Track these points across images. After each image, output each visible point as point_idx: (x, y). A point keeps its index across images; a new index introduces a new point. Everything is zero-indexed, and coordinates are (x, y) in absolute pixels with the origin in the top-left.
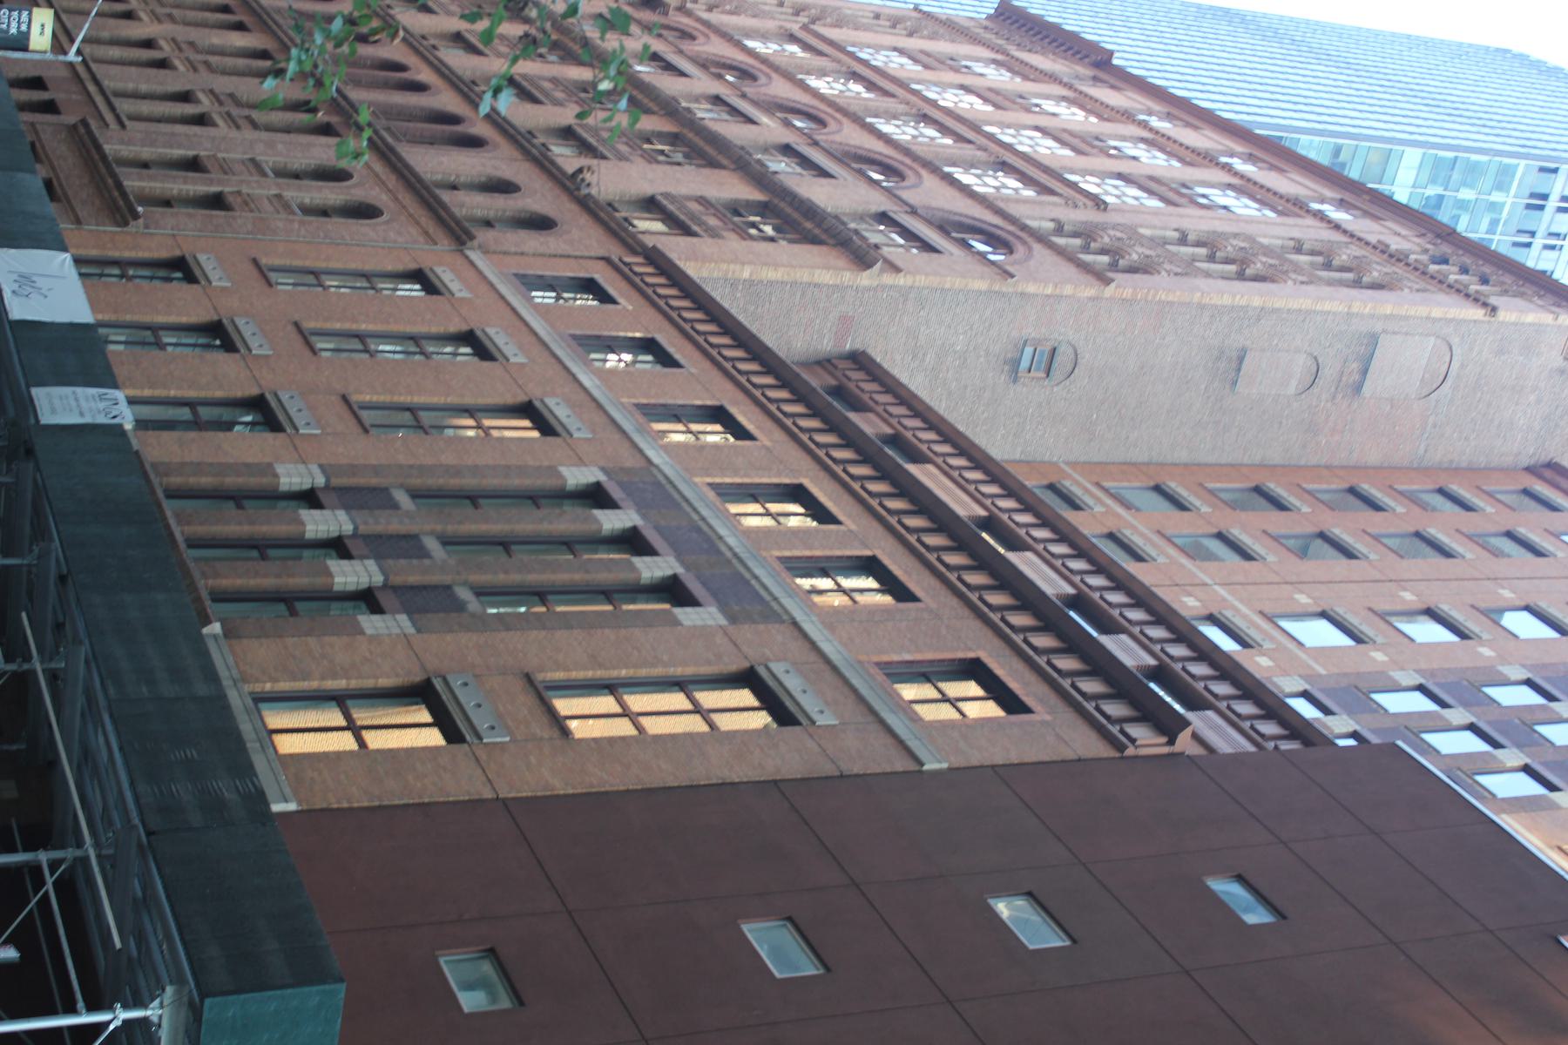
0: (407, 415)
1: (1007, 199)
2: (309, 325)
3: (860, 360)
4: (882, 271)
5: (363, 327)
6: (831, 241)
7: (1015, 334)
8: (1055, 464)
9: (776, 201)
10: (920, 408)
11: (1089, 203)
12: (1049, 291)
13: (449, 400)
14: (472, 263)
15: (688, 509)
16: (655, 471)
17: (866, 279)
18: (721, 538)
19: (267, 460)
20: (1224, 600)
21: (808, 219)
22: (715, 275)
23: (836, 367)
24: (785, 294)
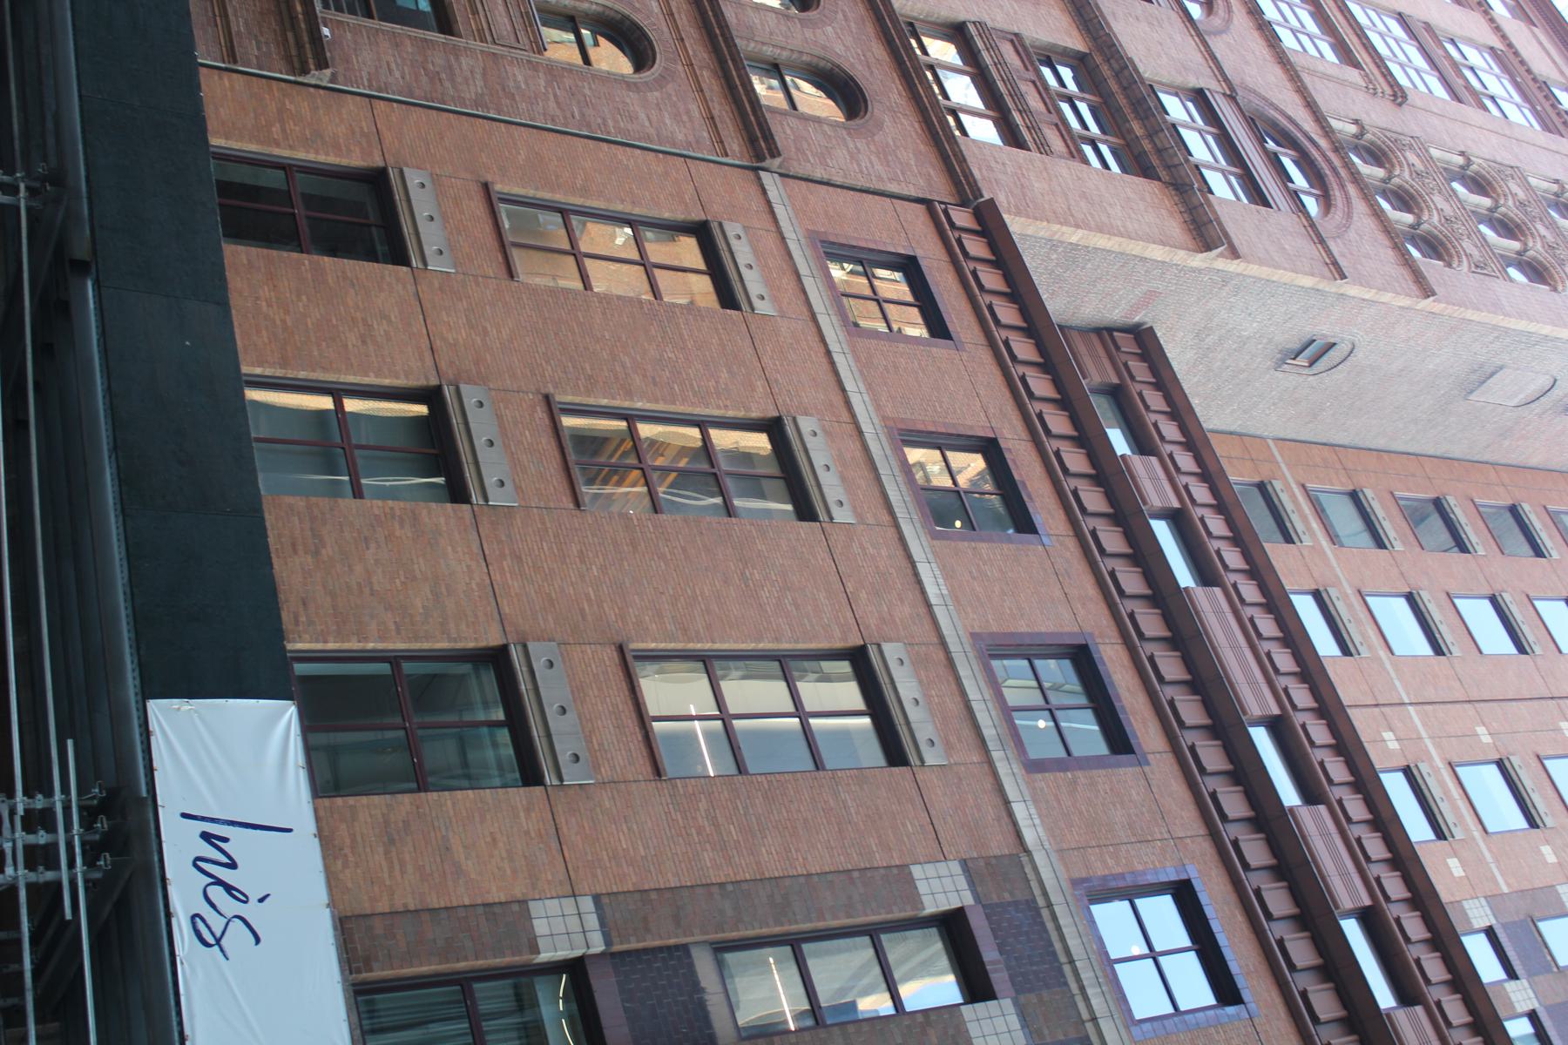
1: (1313, 73)
3: (1144, 340)
4: (1221, 255)
5: (639, 405)
6: (1163, 174)
9: (1098, 59)
10: (1212, 468)
11: (1388, 91)
12: (1367, 297)
13: (761, 646)
14: (764, 192)
15: (1074, 987)
16: (1025, 859)
17: (1199, 260)
19: (518, 892)
20: (1427, 752)
21: (1138, 117)
22: (1041, 234)
23: (1118, 348)
24: (1090, 241)
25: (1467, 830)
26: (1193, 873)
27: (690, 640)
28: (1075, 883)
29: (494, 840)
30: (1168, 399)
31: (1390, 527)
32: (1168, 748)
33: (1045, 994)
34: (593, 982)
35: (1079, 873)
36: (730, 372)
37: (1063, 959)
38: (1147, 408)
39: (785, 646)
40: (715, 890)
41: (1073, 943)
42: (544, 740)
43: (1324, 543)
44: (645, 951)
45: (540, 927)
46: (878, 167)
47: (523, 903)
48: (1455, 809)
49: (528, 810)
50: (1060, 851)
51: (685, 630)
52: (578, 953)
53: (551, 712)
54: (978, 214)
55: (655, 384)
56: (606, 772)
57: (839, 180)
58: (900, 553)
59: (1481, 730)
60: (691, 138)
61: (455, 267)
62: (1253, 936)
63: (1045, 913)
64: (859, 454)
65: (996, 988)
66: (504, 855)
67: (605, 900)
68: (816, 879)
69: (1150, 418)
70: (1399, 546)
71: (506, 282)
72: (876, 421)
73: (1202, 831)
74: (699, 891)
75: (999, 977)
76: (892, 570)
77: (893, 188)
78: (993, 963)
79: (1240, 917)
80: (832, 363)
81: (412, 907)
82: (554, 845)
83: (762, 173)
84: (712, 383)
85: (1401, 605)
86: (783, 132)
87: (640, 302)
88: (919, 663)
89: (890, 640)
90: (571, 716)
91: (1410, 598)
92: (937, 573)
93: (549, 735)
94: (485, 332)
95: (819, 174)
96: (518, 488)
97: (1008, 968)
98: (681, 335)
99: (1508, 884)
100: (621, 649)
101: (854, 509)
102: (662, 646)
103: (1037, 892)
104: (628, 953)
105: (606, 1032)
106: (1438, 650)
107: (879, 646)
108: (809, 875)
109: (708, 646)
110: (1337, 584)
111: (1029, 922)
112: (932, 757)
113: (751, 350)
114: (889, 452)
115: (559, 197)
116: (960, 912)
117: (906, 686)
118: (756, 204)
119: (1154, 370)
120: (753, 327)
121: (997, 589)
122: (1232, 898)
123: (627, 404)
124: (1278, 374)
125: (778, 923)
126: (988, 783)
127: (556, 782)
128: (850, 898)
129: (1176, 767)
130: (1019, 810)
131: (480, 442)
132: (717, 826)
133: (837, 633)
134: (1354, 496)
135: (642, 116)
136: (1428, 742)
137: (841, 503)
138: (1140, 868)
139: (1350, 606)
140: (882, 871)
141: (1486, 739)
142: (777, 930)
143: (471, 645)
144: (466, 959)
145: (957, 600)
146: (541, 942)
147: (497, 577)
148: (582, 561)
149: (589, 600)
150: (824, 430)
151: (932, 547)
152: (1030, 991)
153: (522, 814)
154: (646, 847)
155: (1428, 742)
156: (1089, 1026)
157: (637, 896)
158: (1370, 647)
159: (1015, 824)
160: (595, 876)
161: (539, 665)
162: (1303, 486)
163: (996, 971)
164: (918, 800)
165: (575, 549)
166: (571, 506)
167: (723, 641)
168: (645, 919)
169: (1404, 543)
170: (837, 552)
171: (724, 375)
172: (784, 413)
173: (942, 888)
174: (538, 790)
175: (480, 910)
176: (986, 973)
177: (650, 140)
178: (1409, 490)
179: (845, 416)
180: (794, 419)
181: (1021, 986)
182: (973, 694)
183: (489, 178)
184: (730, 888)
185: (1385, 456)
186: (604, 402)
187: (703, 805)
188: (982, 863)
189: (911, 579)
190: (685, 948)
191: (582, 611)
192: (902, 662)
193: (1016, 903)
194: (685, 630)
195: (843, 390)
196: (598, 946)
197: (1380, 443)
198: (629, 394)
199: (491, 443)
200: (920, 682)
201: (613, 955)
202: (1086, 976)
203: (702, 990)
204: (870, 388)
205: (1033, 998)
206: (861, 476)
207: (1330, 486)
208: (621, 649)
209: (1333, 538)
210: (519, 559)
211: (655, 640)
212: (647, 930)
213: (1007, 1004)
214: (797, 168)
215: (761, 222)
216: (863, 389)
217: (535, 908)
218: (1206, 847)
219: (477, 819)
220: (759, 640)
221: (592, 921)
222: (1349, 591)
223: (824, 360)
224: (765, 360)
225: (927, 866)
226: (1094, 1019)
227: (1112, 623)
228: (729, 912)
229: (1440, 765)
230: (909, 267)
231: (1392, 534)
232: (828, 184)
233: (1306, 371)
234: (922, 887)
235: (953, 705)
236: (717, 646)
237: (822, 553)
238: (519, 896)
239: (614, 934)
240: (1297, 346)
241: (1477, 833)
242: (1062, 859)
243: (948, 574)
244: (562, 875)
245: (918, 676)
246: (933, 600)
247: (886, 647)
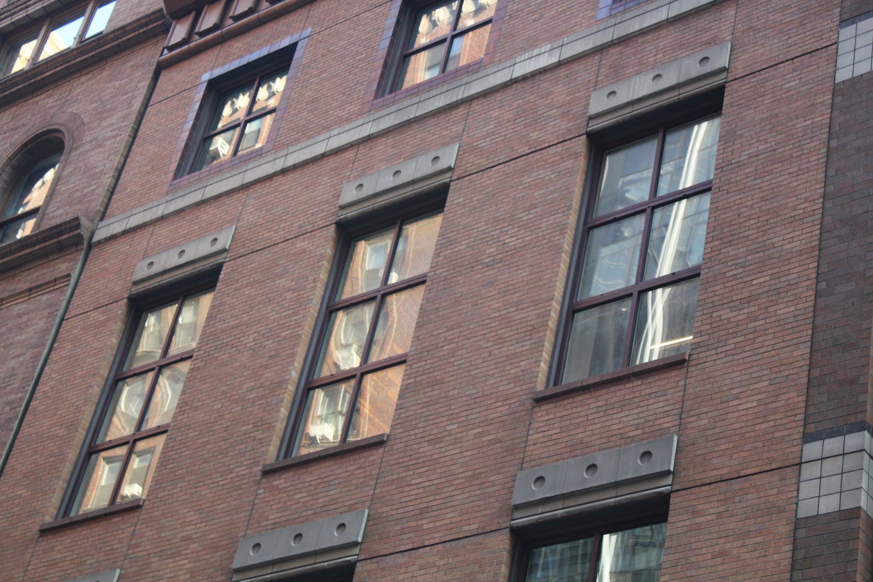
0: (581, 320)
2: (271, 454)
5: (294, 374)
13: (567, 247)
14: (113, 237)
19: (784, 528)
27: (545, 324)
29: (721, 554)
36: (280, 276)
39: (572, 220)
40: (822, 302)
45: (829, 505)
46: (115, 118)
47: (798, 524)
49: (695, 513)
53: (592, 481)
54: (178, 16)
55: (277, 356)
56: (668, 423)
57: (117, 160)
58: (499, 96)
60: (45, 313)
61: (113, 569)
64: (389, 140)
66: (740, 543)
67: (812, 428)
68: (830, 188)
71: (142, 515)
72: (361, 121)
74: (820, 320)
76: (515, 105)
77: (137, 104)
80: (295, 167)
82: (737, 485)
83: (95, 239)
84: (289, 295)
86: (59, 215)
87: (192, 370)
88: (617, 74)
89: (587, 106)
90: (599, 459)
92: (527, 55)
93: (617, 485)
94: (188, 539)
95: (107, 180)
96: (351, 508)
98: (237, 327)
100: (540, 400)
101: (444, 145)
102: (546, 356)
107: (591, 118)
108: (825, 196)
109: (556, 306)
112: (720, 59)
113: (264, 254)
114: (394, 108)
115: (72, 454)
118: (122, 246)
120: (242, 251)
123: (291, 388)
127: (669, 480)
131: (295, 548)
132: (749, 300)
133: (569, 164)
135: (12, 363)
137: (436, 158)
140: (836, 113)
143: (504, 569)
145: (560, 35)
146: (848, 505)
147: (438, 536)
148: (439, 440)
149: (480, 435)
150: (360, 176)
153: (698, 520)
154: (760, 379)
160: (782, 440)
161: (539, 493)
164: (764, 75)
165: (426, 448)
166: (381, 451)
170: (484, 163)
171: (282, 282)
172: (334, 219)
174: (674, 500)
177: (40, 355)
179: (350, 154)
180: (342, 208)
183: (36, 528)
184: (823, 285)
186: (284, 412)
187: (725, 314)
189: (528, 84)
191: (492, 442)
192: (613, 93)
194: (534, 329)
195: (323, 156)
198: (281, 384)
199: (299, 536)
200: (638, 73)
204: (327, 128)
206: (416, 135)
208: (540, 400)
210: (423, 511)
211: (538, 363)
214: (97, 205)
215: (141, 240)
216: (326, 135)
217: (806, 510)
219: (693, 572)
220: (559, 249)
221: (833, 445)
223: (291, 176)
224: (277, 238)
225: (840, 64)
230: (221, 90)
232: (120, 171)
235: (668, 37)
236: (558, 294)
237: (485, 180)
238: (789, 528)
243: (532, 43)
244: (774, 477)
246: (555, 59)
247: (593, 109)
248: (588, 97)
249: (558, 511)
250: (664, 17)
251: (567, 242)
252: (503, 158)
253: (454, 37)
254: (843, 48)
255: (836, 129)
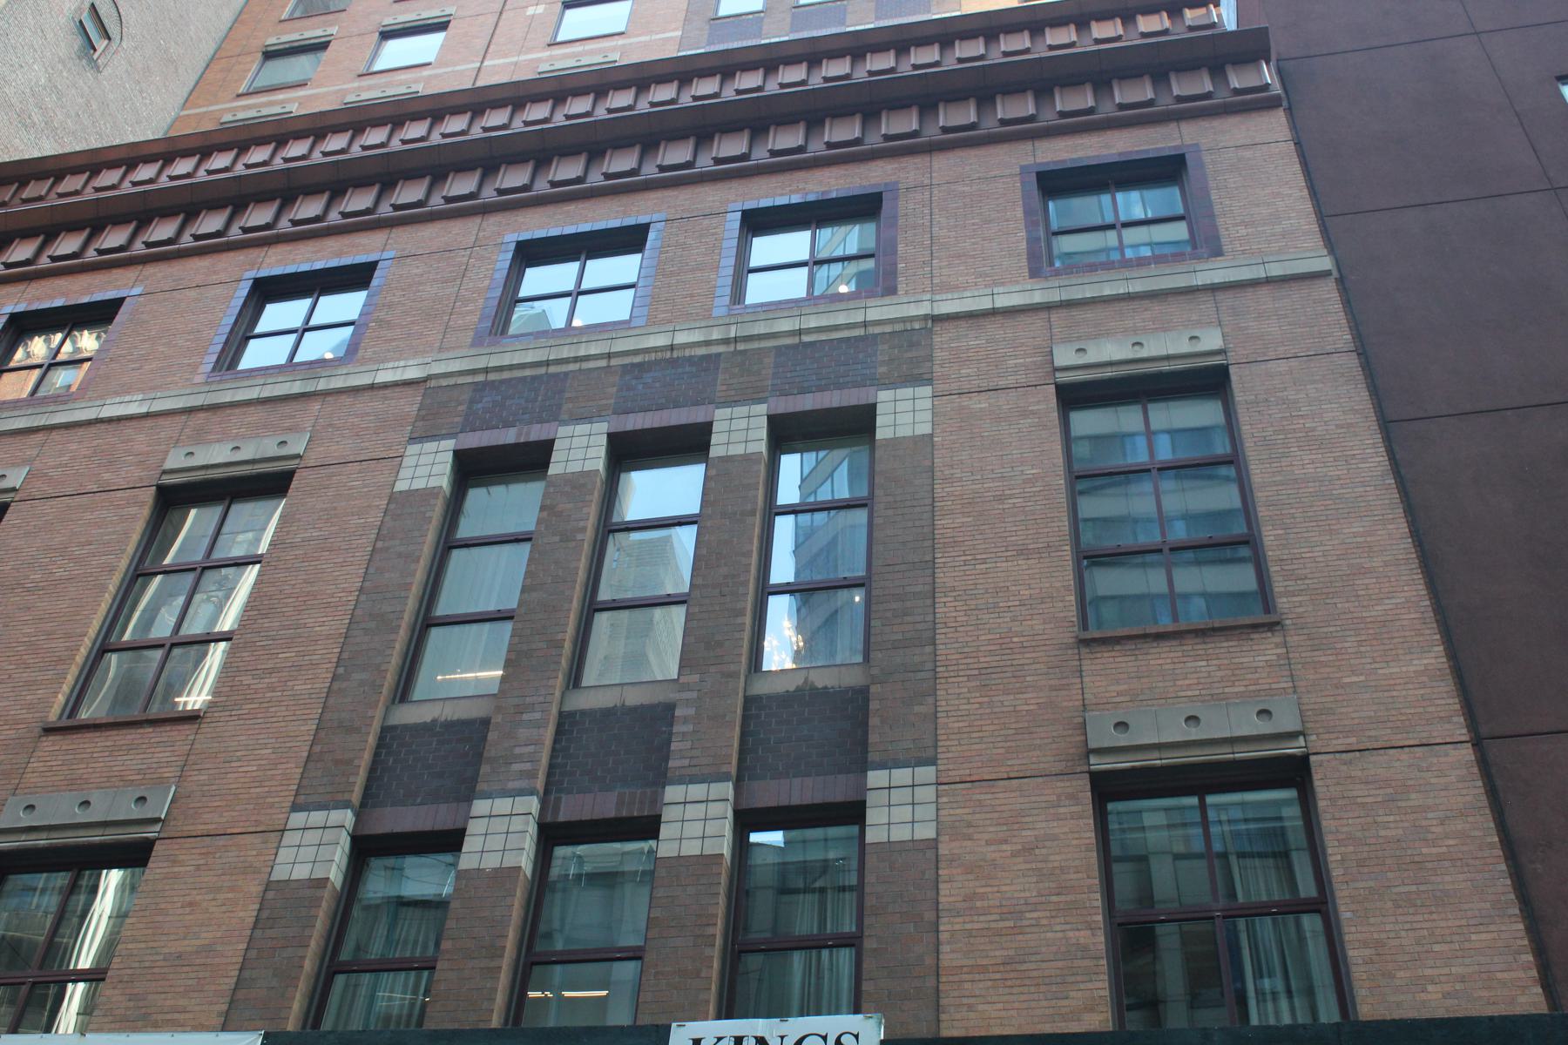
7: (62, 20)
8: (177, 119)
13: (112, 589)
16: (433, 383)
18: (672, 347)
19: (255, 888)
20: (532, 60)
25: (614, 49)
26: (512, 238)
27: (72, 658)
28: (477, 342)
29: (191, 904)
30: (76, 171)
31: (312, 31)
32: (387, 231)
33: (567, 395)
34: (381, 831)
35: (469, 337)
37: (542, 371)
38: (77, 193)
39: (124, 563)
40: (336, 686)
41: (530, 357)
42: (109, 831)
43: (301, 93)
44: (372, 770)
45: (302, 872)
47: (269, 886)
48: (592, 53)
50: (440, 350)
51: (60, 660)
52: (345, 841)
56: (170, 772)
58: (81, 432)
59: (530, 11)
62: (593, 201)
63: (492, 377)
65: (544, 437)
67: (301, 799)
68: (367, 584)
69: (89, 195)
70: (334, 30)
73: (478, 220)
74: (331, 701)
75: (536, 433)
78: (519, 435)
79: (571, 208)
81: (225, 1007)
82: (221, 841)
85: (393, 46)
88: (200, 437)
89: (163, 460)
90: (94, 797)
91: (387, 35)
97: (531, 423)
99: (675, 29)
100: (49, 730)
101: (14, 465)
102: (66, 688)
103: (469, 379)
104: (367, 788)
105: (438, 827)
106: (441, 26)
107: (164, 472)
108: (361, 590)
109: (87, 642)
110: (346, 92)
111: (490, 393)
112: (297, 446)
116: (459, 455)
117: (216, 454)
119: (40, 176)
121: (161, 349)
122: (550, 210)
124: (105, 73)
125: (395, 630)
126: (346, 400)
127: (158, 827)
128: (400, 555)
129: (408, 229)
130: (384, 377)
132: (271, 671)
133: (133, 510)
134: (269, 55)
136: (523, 58)
138: (487, 282)
139: (369, 88)
140: (387, 518)
141: (540, 9)
142: (402, 634)
144: (303, 958)
145: (153, 388)
146: (319, 874)
151: (90, 399)
152: (559, 407)
155: (523, 58)
156: (614, 362)
157: (311, 765)
158: (416, 81)
159: (395, 384)
160: (272, 806)
161: (26, 820)
162: (239, 96)
163: (528, 434)
167: (88, 625)
168: (337, 762)
169: (331, 25)
170: (51, 491)
173: (429, 467)
174: (158, 847)
175: (258, 933)
176: (527, 444)
178: (284, 7)
181: (553, 415)
182: (254, 394)
184: (341, 670)
185: (243, 16)
187: (247, 680)
188: (420, 424)
189: (112, 427)
190: (386, 731)
193: (472, 401)
194: (60, 660)
196: (347, 817)
197: (227, 16)
200: (218, 441)
201: (363, 804)
202: (566, 353)
203: (434, 721)
205: (567, 407)
207: (252, 72)
208: (49, 730)
209: (302, 85)
212: (349, 762)
213: (563, 431)
217: (280, 874)
218: (493, 222)
219: (160, 918)
220: (104, 588)
221: (317, 817)
222: (356, 84)
225: (401, 475)
226: (609, 356)
227: (246, 251)
228: (364, 676)
229: (547, 53)
231: (319, 32)
233: (114, 45)
234: (419, 484)
236: (92, 632)
237: (50, 508)
238: (261, 888)
239: (340, 797)
240: (79, 41)
241: (620, 41)
242: (448, 349)
245: (210, 442)
246: (144, 410)
247: (168, 465)
248: (166, 453)
249: (42, 841)
250: (255, 396)
251: (113, 584)
252: (69, 491)
253: (51, 366)
254: (407, 462)
255: (384, 532)
